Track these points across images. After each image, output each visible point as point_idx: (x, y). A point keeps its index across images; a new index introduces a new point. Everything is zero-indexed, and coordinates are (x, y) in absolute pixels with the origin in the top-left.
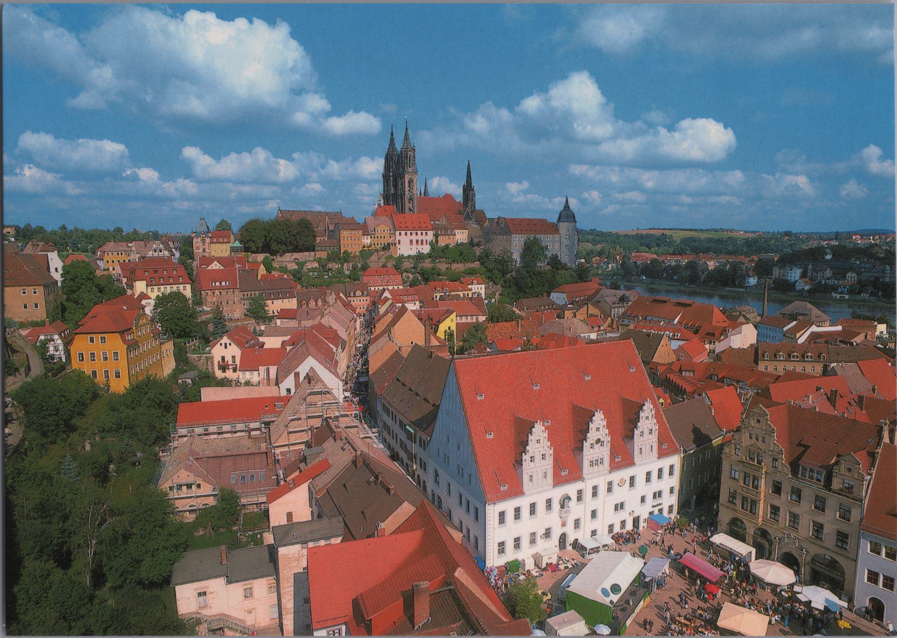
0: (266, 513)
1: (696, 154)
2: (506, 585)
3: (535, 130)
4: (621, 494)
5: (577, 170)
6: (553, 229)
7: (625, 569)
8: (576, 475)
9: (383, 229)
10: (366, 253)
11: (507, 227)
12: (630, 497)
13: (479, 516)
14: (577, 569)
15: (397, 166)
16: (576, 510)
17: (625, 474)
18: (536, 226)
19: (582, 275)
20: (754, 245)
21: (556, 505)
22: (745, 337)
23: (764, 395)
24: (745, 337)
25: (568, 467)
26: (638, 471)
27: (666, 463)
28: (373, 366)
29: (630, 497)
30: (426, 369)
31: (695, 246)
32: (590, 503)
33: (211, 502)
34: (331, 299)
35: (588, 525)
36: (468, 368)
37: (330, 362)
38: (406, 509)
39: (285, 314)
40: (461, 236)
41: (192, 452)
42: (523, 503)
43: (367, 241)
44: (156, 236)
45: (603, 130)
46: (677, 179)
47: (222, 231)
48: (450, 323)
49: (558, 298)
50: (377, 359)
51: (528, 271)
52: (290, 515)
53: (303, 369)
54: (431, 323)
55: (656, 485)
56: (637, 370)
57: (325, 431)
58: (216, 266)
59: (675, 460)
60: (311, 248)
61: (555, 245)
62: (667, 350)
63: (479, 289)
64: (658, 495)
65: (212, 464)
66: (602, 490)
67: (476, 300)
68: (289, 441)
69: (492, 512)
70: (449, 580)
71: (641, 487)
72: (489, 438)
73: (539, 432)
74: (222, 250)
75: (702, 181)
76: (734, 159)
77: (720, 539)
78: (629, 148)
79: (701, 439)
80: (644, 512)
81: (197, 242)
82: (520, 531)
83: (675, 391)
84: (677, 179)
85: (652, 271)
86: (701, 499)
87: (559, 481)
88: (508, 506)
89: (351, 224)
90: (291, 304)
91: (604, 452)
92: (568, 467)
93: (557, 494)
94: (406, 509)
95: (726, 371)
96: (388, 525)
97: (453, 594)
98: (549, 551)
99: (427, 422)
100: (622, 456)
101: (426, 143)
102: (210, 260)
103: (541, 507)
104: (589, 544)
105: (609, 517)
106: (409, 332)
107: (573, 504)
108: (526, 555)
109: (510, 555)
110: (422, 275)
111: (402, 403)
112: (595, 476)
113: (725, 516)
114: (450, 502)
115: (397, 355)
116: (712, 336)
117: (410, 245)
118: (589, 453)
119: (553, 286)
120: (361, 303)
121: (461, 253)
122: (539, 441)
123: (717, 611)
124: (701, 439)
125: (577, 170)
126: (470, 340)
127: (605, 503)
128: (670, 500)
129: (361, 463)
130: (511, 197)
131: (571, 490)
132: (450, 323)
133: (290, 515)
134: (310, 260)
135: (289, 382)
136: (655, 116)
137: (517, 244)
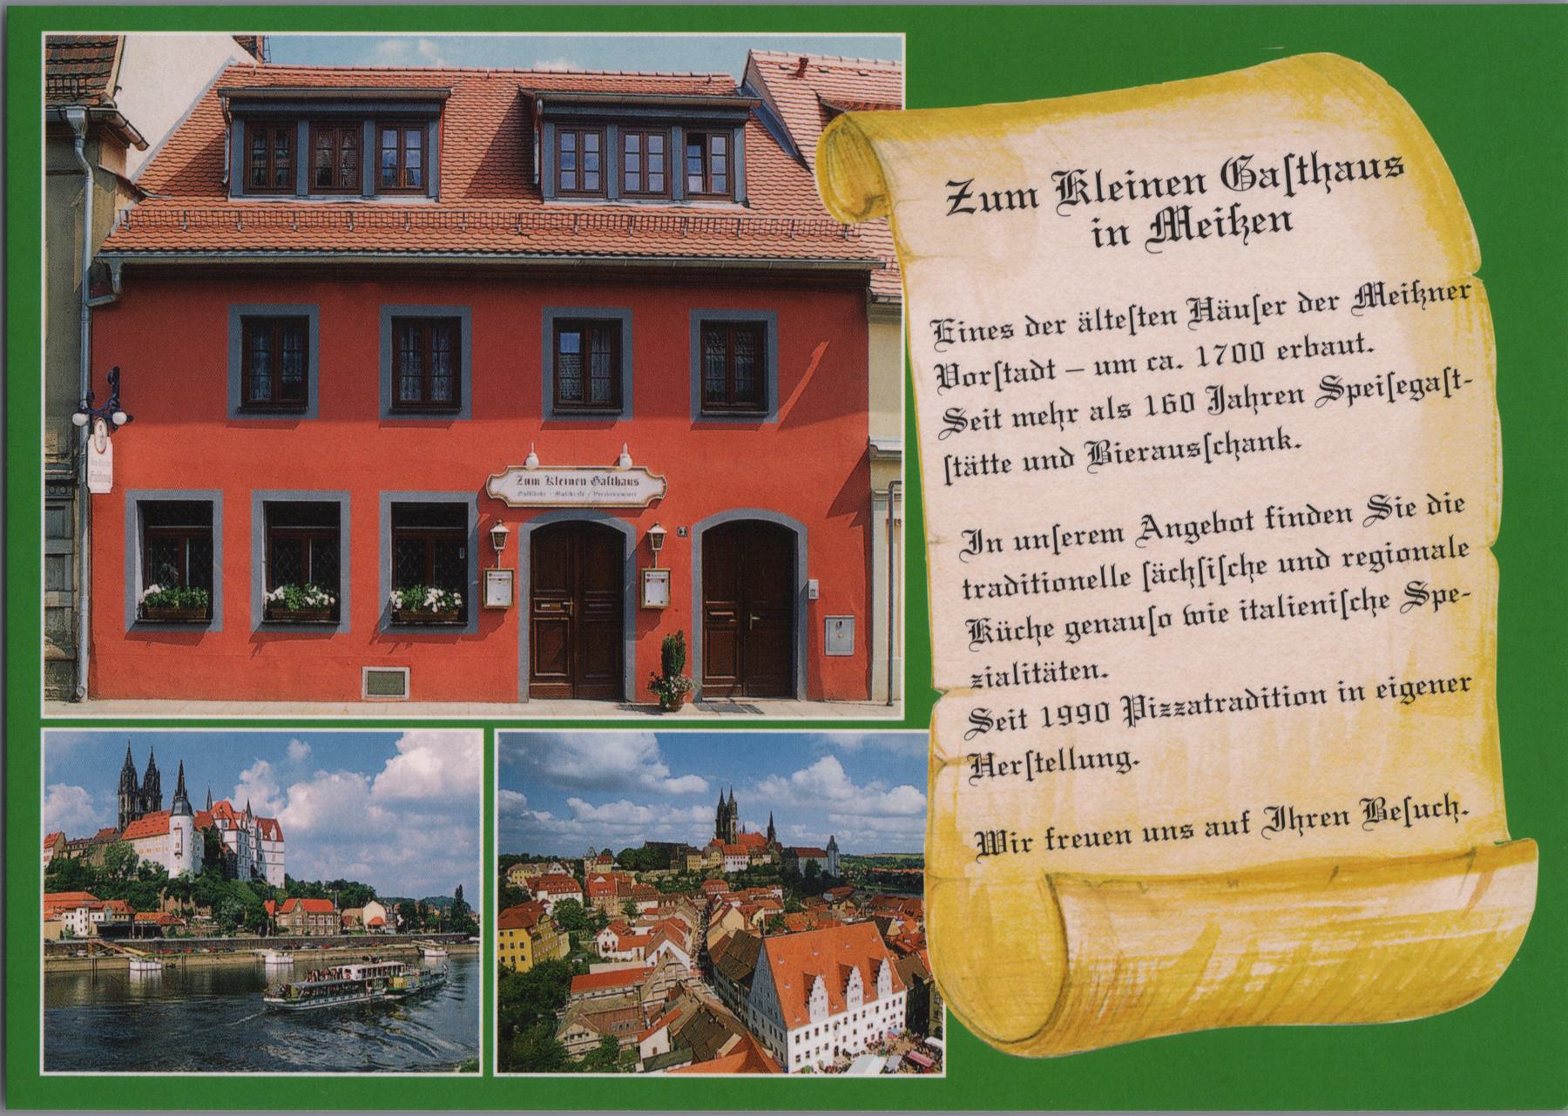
0: (638, 1049)
5: (834, 818)
6: (825, 854)
8: (843, 1008)
10: (704, 871)
11: (793, 853)
12: (876, 1020)
13: (783, 1039)
15: (726, 813)
16: (844, 1030)
17: (873, 1005)
21: (831, 1028)
25: (837, 1003)
26: (881, 1003)
27: (896, 997)
28: (711, 943)
29: (876, 1020)
30: (747, 946)
32: (852, 1025)
33: (597, 1045)
34: (681, 900)
35: (851, 1039)
36: (773, 944)
37: (681, 943)
38: (735, 1039)
39: (649, 912)
40: (767, 859)
41: (581, 1011)
42: (811, 1028)
43: (705, 862)
44: (556, 859)
47: (606, 856)
48: (760, 915)
49: (828, 897)
50: (711, 943)
52: (655, 1050)
53: (662, 948)
54: (747, 914)
55: (892, 1010)
57: (679, 990)
58: (600, 879)
59: (903, 995)
60: (668, 867)
61: (823, 864)
63: (779, 892)
64: (893, 1017)
65: (596, 1018)
66: (859, 1017)
67: (777, 899)
68: (654, 997)
69: (791, 1036)
71: (883, 1013)
72: (787, 990)
73: (819, 983)
74: (605, 869)
78: (863, 804)
81: (587, 863)
87: (832, 1012)
88: (801, 1031)
89: (694, 851)
90: (654, 904)
91: (859, 992)
92: (837, 1003)
93: (831, 1021)
94: (735, 1039)
96: (724, 1051)
98: (828, 1058)
99: (748, 980)
100: (870, 994)
101: (742, 798)
102: (598, 875)
103: (822, 1030)
104: (852, 1051)
105: (864, 1033)
106: (734, 922)
107: (841, 1027)
108: (813, 1062)
109: (804, 1063)
110: (741, 882)
111: (732, 968)
115: (726, 937)
117: (731, 866)
118: (851, 993)
119: (826, 890)
120: (701, 902)
121: (767, 870)
124: (917, 980)
125: (834, 818)
126: (774, 925)
127: (861, 1024)
128: (901, 1019)
130: (793, 835)
131: (840, 1017)
132: (760, 915)
133: (655, 1050)
134: (667, 875)
135: (653, 958)
136: (877, 784)
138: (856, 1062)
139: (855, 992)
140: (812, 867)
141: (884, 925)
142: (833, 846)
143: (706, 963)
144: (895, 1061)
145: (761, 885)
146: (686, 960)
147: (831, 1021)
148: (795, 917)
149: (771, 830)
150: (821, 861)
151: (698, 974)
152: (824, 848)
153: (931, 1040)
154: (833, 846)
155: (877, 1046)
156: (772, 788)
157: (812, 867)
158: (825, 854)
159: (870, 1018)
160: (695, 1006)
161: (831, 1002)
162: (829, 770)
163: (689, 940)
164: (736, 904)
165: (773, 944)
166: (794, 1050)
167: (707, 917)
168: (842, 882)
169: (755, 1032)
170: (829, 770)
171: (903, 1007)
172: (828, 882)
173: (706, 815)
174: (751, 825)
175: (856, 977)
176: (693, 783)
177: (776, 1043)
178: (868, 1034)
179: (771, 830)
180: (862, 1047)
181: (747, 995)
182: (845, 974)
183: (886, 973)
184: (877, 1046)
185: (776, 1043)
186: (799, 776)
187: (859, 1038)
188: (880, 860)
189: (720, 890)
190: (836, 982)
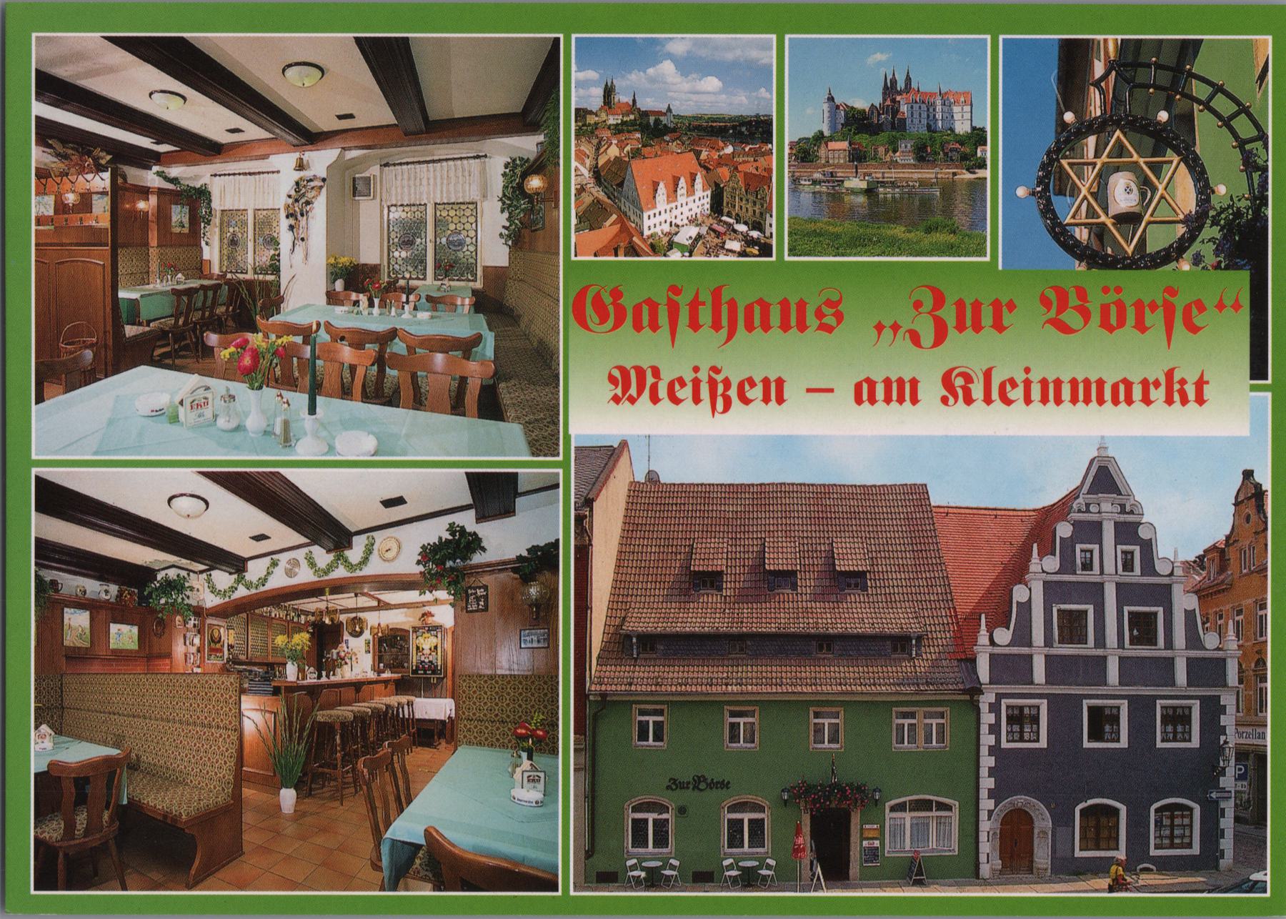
1: (710, 89)
3: (653, 80)
4: (691, 205)
5: (670, 94)
6: (665, 114)
7: (693, 231)
8: (675, 199)
11: (646, 114)
13: (641, 217)
15: (609, 92)
17: (692, 198)
18: (660, 113)
20: (731, 119)
22: (729, 150)
23: (736, 168)
28: (601, 163)
31: (713, 119)
36: (636, 165)
40: (632, 117)
42: (657, 211)
45: (678, 79)
46: (704, 98)
48: (628, 148)
49: (667, 138)
51: (653, 129)
54: (622, 149)
56: (695, 161)
59: (709, 193)
61: (664, 120)
62: (704, 155)
63: (638, 135)
67: (637, 139)
69: (645, 215)
70: (631, 242)
72: (643, 190)
73: (662, 185)
75: (712, 98)
76: (723, 91)
78: (686, 86)
79: (717, 185)
82: (654, 222)
84: (704, 98)
85: (698, 128)
86: (717, 206)
87: (669, 202)
88: (651, 213)
89: (591, 112)
91: (684, 191)
94: (614, 217)
95: (722, 161)
97: (633, 247)
98: (666, 228)
99: (621, 185)
100: (691, 190)
101: (618, 83)
104: (680, 223)
106: (613, 152)
108: (658, 230)
109: (653, 230)
110: (618, 130)
111: (611, 178)
112: (682, 199)
113: (726, 210)
116: (718, 150)
117: (612, 120)
118: (679, 192)
120: (595, 141)
121: (633, 123)
122: (662, 189)
124: (717, 185)
125: (670, 94)
126: (636, 154)
127: (685, 209)
129: (597, 202)
130: (646, 104)
131: (673, 205)
132: (628, 148)
136: (694, 76)
137: (652, 119)
138: (682, 230)
139: (682, 189)
140: (657, 122)
141: (698, 154)
142: (669, 110)
143: (597, 173)
144: (704, 230)
145: (629, 132)
146: (585, 172)
147: (668, 208)
148: (646, 151)
149: (634, 101)
150: (662, 118)
151: (592, 181)
152: (664, 111)
153: (724, 218)
154: (669, 110)
155: (693, 221)
157: (657, 122)
158: (665, 114)
159: (691, 205)
161: (668, 197)
162: (667, 67)
163: (588, 162)
164: (615, 142)
165: (636, 165)
166: (647, 223)
167: (598, 149)
168: (674, 130)
170: (667, 67)
171: (709, 200)
172: (667, 130)
173: (599, 92)
174: (623, 98)
175: (682, 182)
176: (591, 74)
177: (637, 220)
178: (689, 214)
179: (634, 101)
180: (686, 221)
181: (620, 193)
182: (676, 181)
183: (699, 180)
184: (693, 221)
185: (637, 220)
186: (651, 71)
187: (684, 217)
188: (696, 118)
189: (606, 134)
190: (671, 186)
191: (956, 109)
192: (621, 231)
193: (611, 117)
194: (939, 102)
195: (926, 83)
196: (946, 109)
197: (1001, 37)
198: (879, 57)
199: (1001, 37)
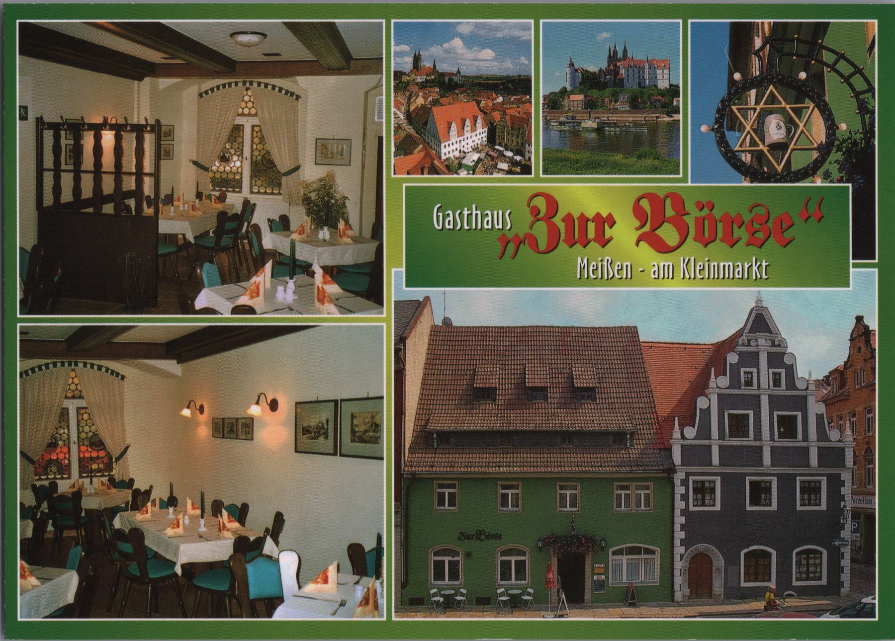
1: (487, 58)
2: (561, 124)
3: (447, 51)
4: (474, 138)
5: (459, 61)
6: (456, 75)
7: (476, 157)
8: (463, 135)
9: (413, 75)
10: (408, 81)
11: (443, 75)
12: (476, 139)
13: (439, 146)
14: (464, 157)
15: (417, 59)
16: (463, 143)
18: (452, 74)
19: (462, 86)
20: (502, 78)
22: (500, 99)
23: (505, 112)
24: (500, 99)
25: (461, 132)
26: (478, 132)
29: (476, 139)
30: (425, 111)
31: (488, 79)
35: (466, 146)
36: (435, 110)
40: (433, 77)
42: (450, 142)
45: (465, 51)
46: (482, 63)
48: (430, 99)
51: (448, 85)
54: (425, 98)
59: (486, 129)
61: (455, 78)
62: (483, 104)
69: (443, 146)
70: (433, 164)
72: (441, 128)
73: (454, 124)
75: (488, 64)
76: (495, 59)
77: (497, 147)
78: (470, 56)
79: (491, 124)
80: (479, 142)
82: (449, 150)
83: (485, 113)
85: (479, 84)
86: (492, 139)
88: (447, 144)
89: (404, 74)
91: (469, 128)
92: (461, 132)
93: (458, 140)
94: (421, 146)
95: (495, 108)
97: (434, 167)
98: (457, 154)
99: (426, 123)
100: (474, 129)
104: (466, 150)
105: (471, 144)
106: (420, 101)
108: (451, 155)
109: (448, 156)
110: (423, 86)
111: (420, 120)
113: (498, 142)
114: (432, 144)
116: (493, 100)
117: (419, 79)
118: (466, 129)
120: (407, 94)
121: (433, 81)
123: (497, 164)
124: (491, 124)
126: (435, 102)
128: (485, 139)
129: (409, 136)
130: (443, 67)
131: (462, 138)
136: (476, 48)
137: (447, 78)
138: (468, 155)
139: (467, 128)
140: (451, 80)
141: (478, 103)
142: (459, 72)
143: (409, 116)
144: (483, 155)
146: (402, 116)
147: (458, 140)
149: (434, 66)
150: (454, 78)
153: (497, 147)
154: (459, 72)
155: (476, 149)
156: (435, 50)
157: (451, 80)
158: (456, 75)
160: (405, 134)
162: (457, 42)
163: (403, 109)
164: (421, 94)
165: (435, 110)
166: (443, 151)
167: (409, 99)
168: (462, 86)
169: (428, 144)
170: (457, 42)
173: (409, 60)
174: (427, 64)
175: (468, 122)
176: (405, 48)
178: (473, 144)
179: (434, 66)
180: (470, 149)
183: (479, 121)
184: (476, 149)
186: (446, 45)
187: (469, 146)
188: (477, 77)
189: (414, 89)
190: (461, 126)
191: (659, 71)
192: (425, 157)
193: (418, 77)
194: (647, 66)
195: (637, 54)
196: (651, 71)
197: (690, 21)
198: (605, 35)
199: (690, 21)
